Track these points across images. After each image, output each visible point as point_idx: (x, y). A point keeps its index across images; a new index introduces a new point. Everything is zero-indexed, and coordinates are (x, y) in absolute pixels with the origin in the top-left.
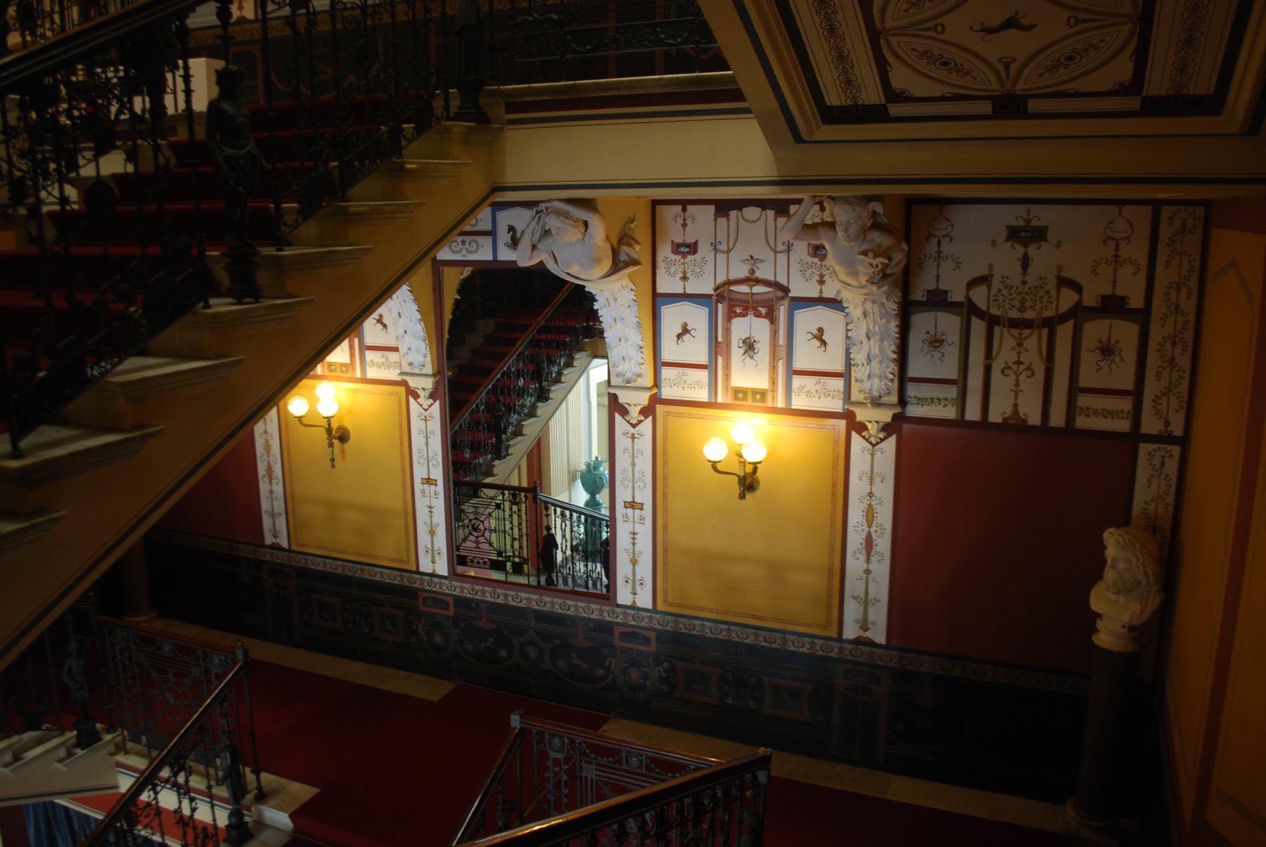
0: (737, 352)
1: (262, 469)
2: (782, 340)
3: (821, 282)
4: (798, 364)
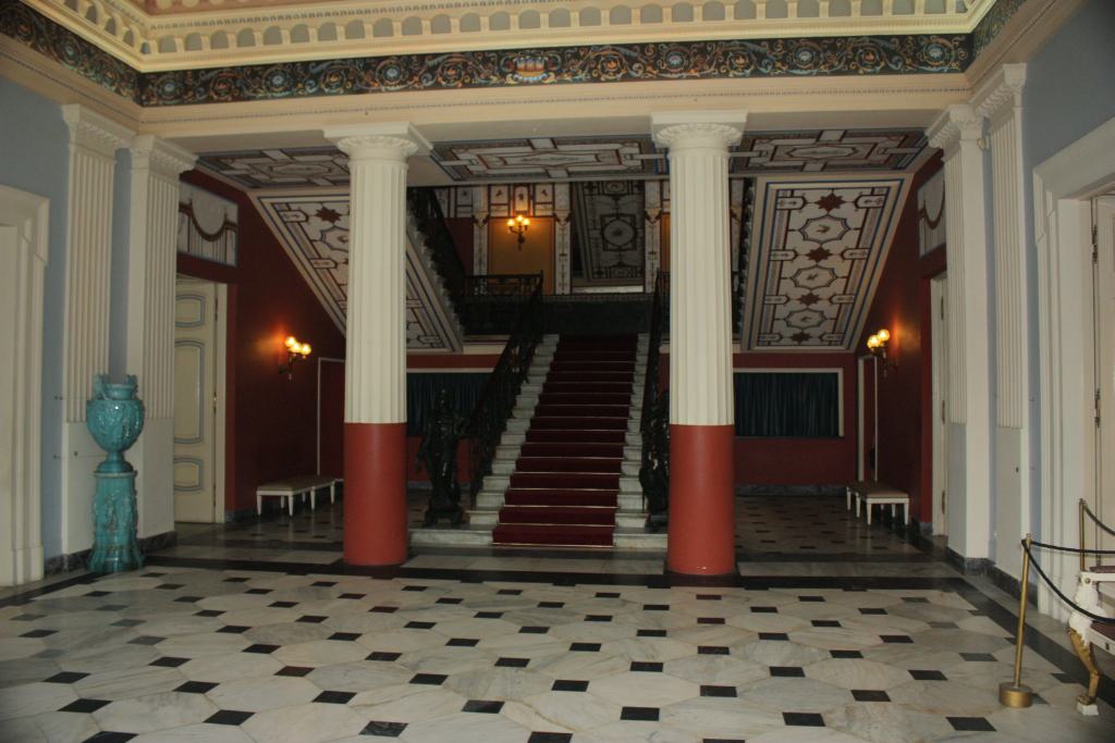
1: (476, 260)
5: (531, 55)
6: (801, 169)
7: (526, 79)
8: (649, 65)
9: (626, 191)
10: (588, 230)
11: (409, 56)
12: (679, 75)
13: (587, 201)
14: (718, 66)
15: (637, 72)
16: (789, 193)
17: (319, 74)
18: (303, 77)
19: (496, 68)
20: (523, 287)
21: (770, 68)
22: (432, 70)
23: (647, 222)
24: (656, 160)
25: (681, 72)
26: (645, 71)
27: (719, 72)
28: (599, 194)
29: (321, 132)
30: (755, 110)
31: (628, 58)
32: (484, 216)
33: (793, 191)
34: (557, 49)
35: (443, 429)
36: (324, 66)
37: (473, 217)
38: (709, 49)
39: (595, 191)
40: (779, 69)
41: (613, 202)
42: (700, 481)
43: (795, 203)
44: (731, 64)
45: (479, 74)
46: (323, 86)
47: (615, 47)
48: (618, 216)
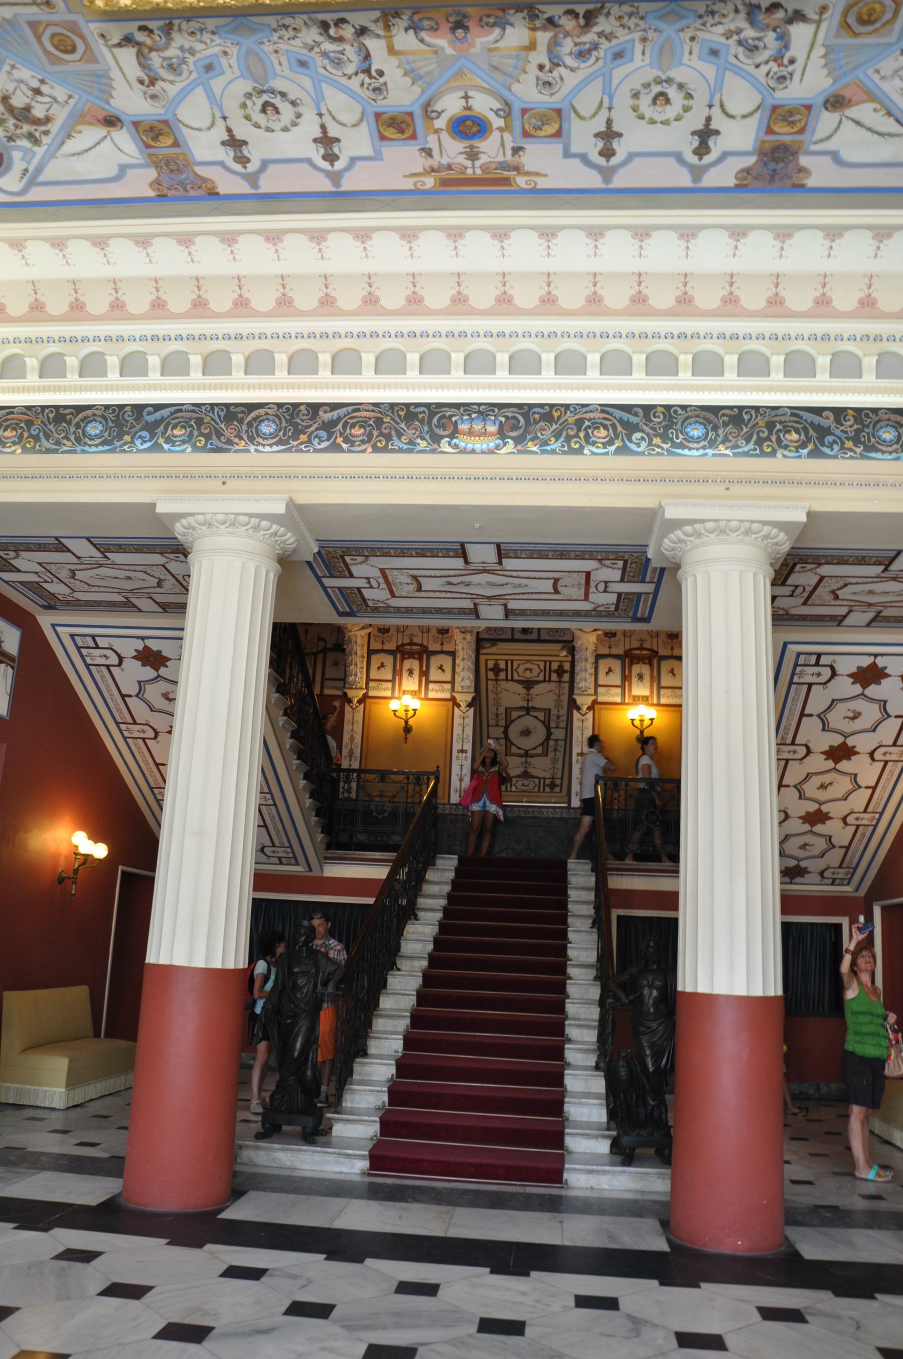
0: (635, 679)
2: (655, 674)
3: (672, 649)
4: (663, 684)
5: (479, 412)
6: (838, 621)
7: (470, 446)
8: (656, 436)
9: (541, 678)
10: (488, 726)
11: (296, 406)
12: (701, 452)
13: (490, 688)
14: (760, 442)
15: (638, 445)
16: (813, 659)
17: (157, 423)
18: (133, 427)
19: (426, 428)
20: (411, 787)
21: (836, 447)
22: (328, 427)
23: (575, 711)
24: (639, 595)
25: (704, 448)
26: (650, 444)
27: (761, 450)
28: (507, 679)
29: (154, 505)
30: (818, 507)
31: (626, 425)
32: (361, 693)
33: (819, 655)
34: (519, 406)
35: (301, 981)
36: (165, 412)
37: (345, 694)
38: (746, 417)
39: (502, 675)
40: (851, 450)
41: (525, 691)
42: (728, 1085)
43: (819, 675)
44: (779, 441)
45: (399, 435)
46: (161, 441)
47: (605, 408)
48: (528, 710)
